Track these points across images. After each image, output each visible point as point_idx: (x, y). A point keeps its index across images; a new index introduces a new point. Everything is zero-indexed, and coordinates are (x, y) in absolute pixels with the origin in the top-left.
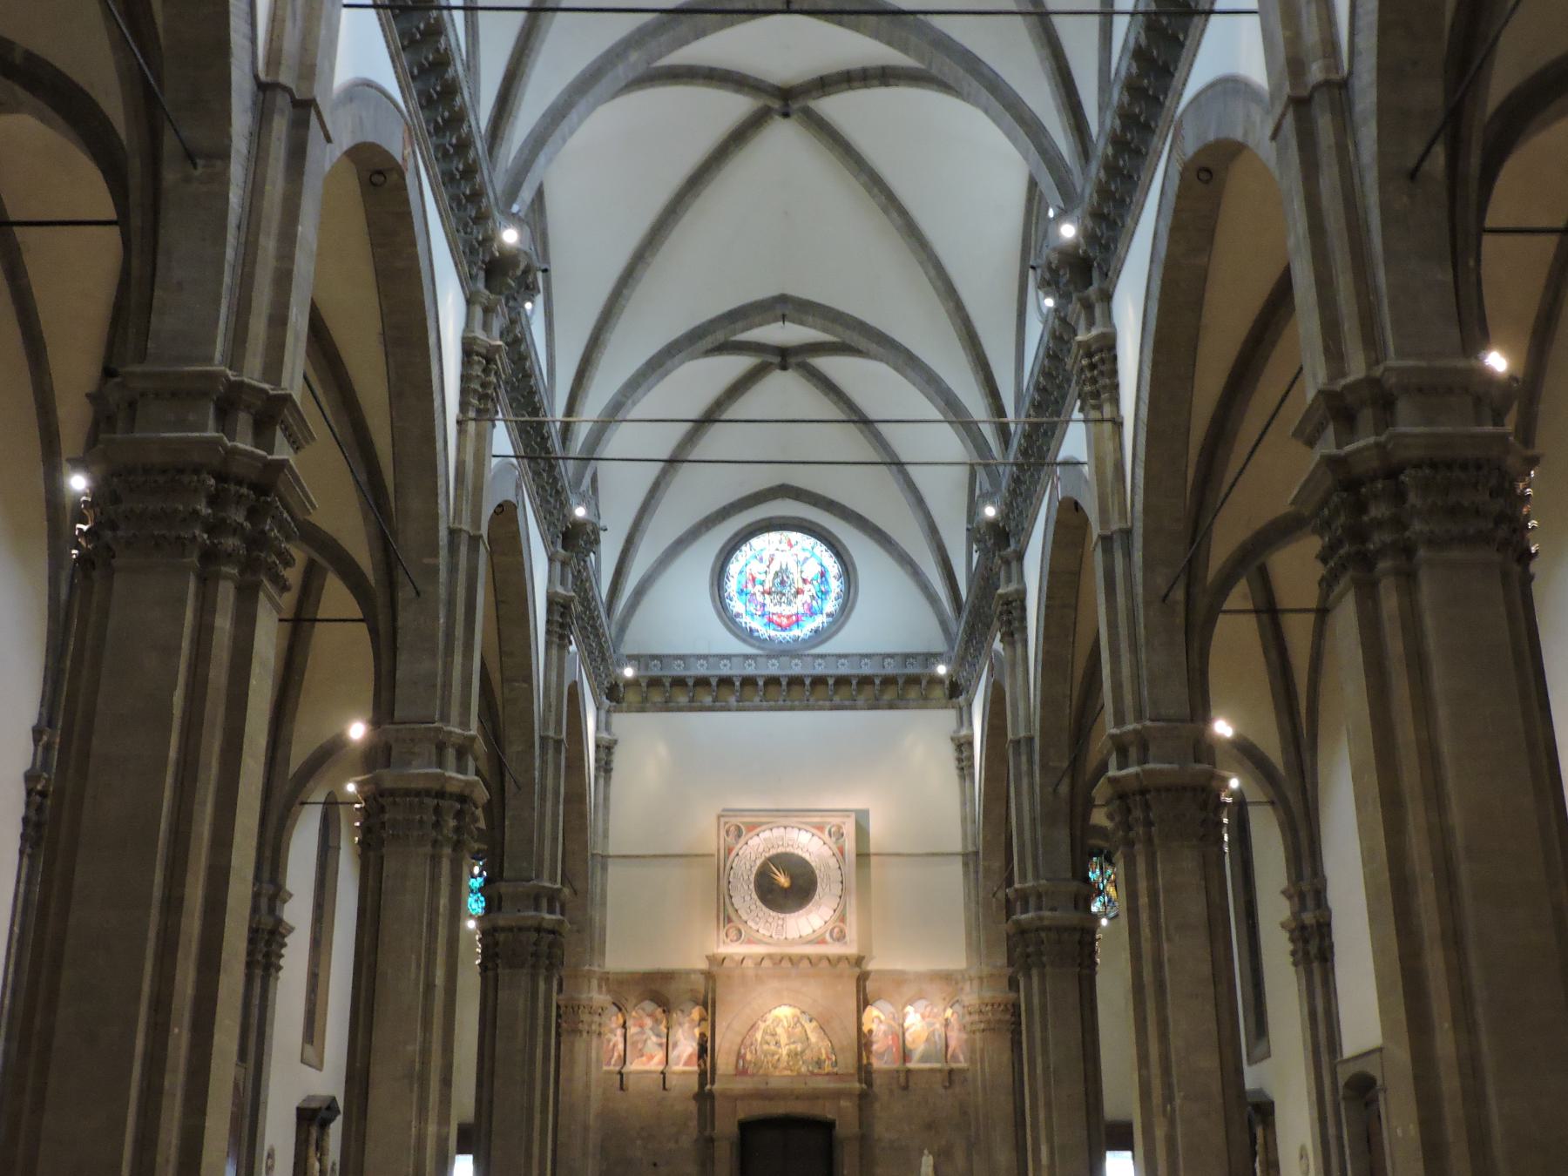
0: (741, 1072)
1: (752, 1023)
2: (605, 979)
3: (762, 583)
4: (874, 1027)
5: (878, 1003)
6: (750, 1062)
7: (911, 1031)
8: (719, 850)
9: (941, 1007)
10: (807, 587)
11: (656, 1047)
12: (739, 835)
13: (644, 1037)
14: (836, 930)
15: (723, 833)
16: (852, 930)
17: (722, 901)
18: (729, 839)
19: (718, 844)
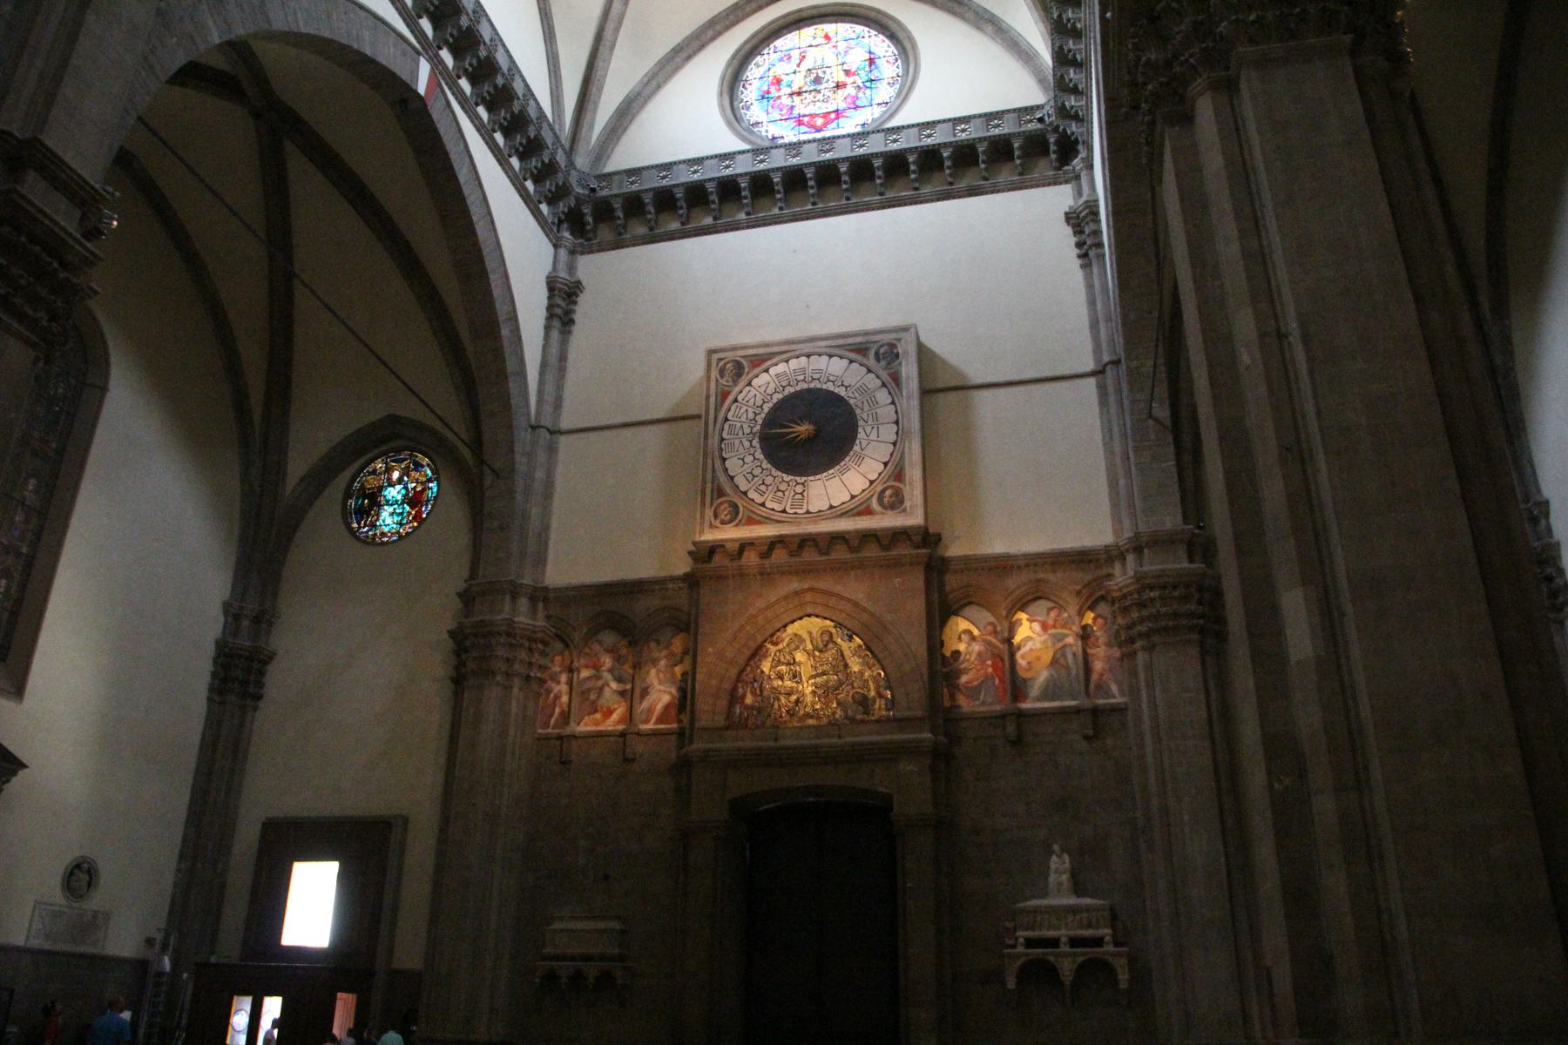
0: (733, 724)
1: (753, 645)
2: (541, 596)
3: (790, 86)
4: (962, 647)
5: (968, 611)
6: (752, 707)
7: (1023, 650)
8: (708, 397)
9: (1073, 609)
10: (849, 80)
11: (617, 698)
12: (739, 370)
13: (600, 683)
14: (888, 493)
15: (714, 374)
16: (914, 492)
17: (710, 466)
18: (723, 382)
19: (708, 388)
